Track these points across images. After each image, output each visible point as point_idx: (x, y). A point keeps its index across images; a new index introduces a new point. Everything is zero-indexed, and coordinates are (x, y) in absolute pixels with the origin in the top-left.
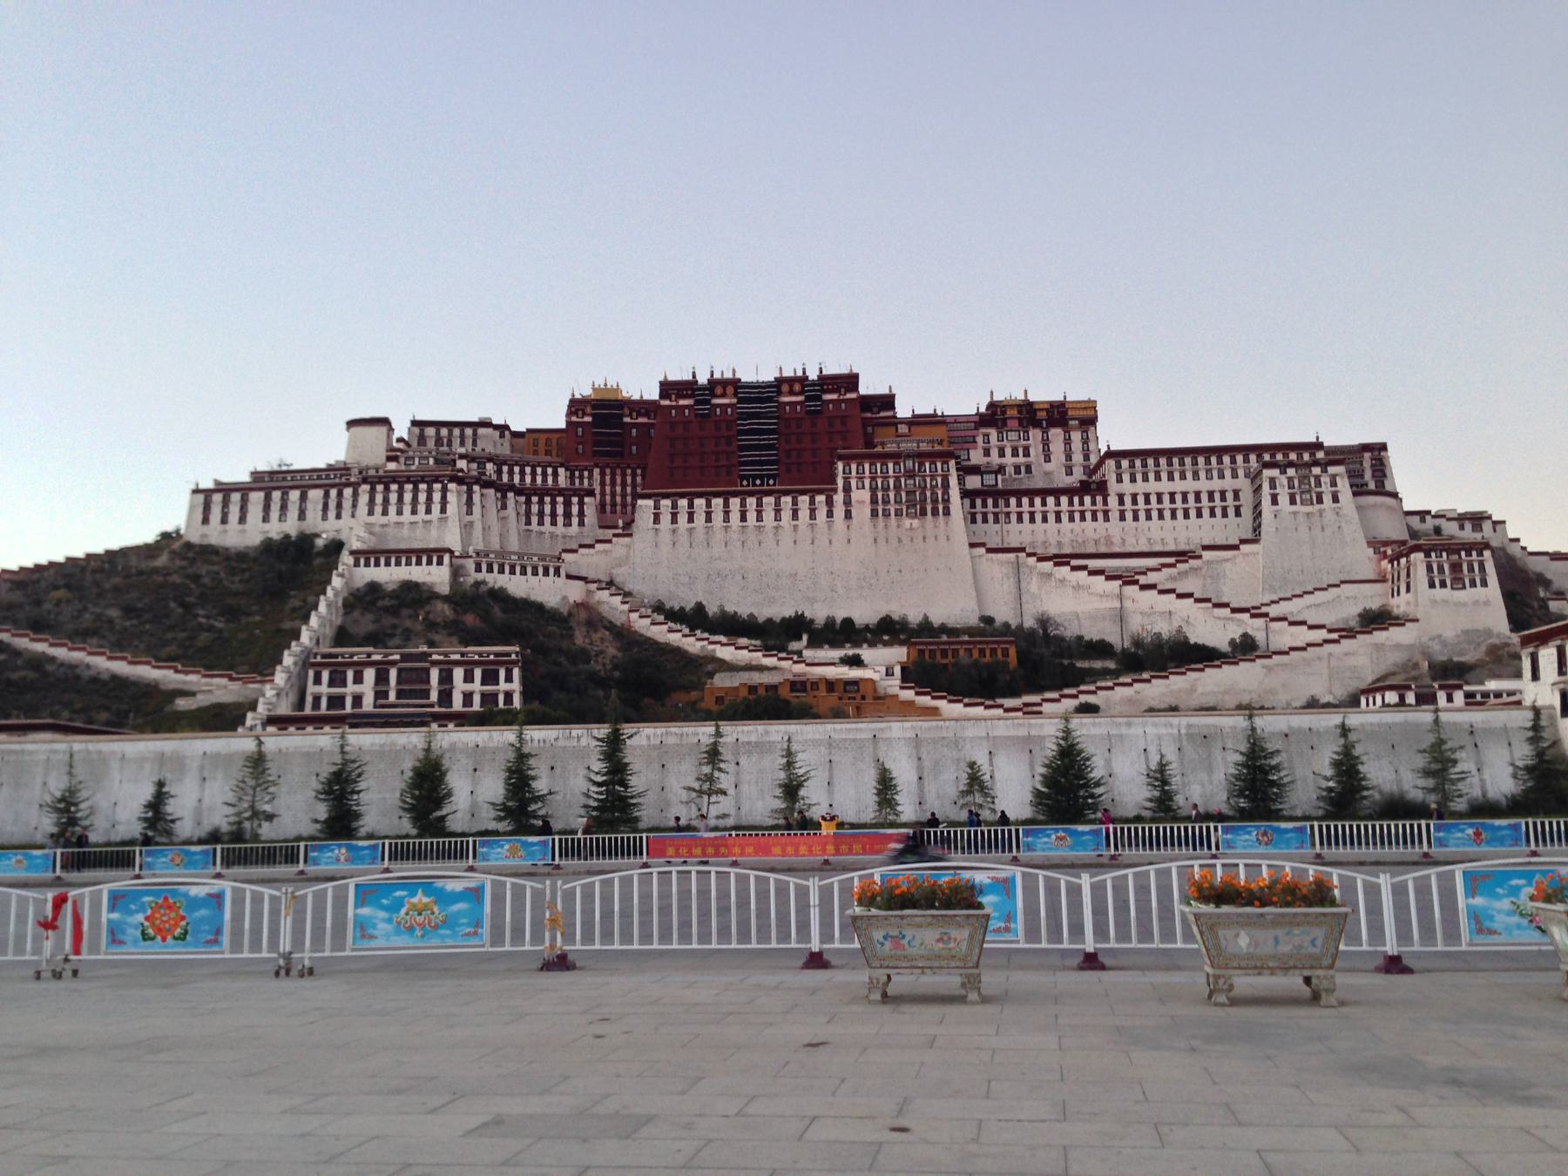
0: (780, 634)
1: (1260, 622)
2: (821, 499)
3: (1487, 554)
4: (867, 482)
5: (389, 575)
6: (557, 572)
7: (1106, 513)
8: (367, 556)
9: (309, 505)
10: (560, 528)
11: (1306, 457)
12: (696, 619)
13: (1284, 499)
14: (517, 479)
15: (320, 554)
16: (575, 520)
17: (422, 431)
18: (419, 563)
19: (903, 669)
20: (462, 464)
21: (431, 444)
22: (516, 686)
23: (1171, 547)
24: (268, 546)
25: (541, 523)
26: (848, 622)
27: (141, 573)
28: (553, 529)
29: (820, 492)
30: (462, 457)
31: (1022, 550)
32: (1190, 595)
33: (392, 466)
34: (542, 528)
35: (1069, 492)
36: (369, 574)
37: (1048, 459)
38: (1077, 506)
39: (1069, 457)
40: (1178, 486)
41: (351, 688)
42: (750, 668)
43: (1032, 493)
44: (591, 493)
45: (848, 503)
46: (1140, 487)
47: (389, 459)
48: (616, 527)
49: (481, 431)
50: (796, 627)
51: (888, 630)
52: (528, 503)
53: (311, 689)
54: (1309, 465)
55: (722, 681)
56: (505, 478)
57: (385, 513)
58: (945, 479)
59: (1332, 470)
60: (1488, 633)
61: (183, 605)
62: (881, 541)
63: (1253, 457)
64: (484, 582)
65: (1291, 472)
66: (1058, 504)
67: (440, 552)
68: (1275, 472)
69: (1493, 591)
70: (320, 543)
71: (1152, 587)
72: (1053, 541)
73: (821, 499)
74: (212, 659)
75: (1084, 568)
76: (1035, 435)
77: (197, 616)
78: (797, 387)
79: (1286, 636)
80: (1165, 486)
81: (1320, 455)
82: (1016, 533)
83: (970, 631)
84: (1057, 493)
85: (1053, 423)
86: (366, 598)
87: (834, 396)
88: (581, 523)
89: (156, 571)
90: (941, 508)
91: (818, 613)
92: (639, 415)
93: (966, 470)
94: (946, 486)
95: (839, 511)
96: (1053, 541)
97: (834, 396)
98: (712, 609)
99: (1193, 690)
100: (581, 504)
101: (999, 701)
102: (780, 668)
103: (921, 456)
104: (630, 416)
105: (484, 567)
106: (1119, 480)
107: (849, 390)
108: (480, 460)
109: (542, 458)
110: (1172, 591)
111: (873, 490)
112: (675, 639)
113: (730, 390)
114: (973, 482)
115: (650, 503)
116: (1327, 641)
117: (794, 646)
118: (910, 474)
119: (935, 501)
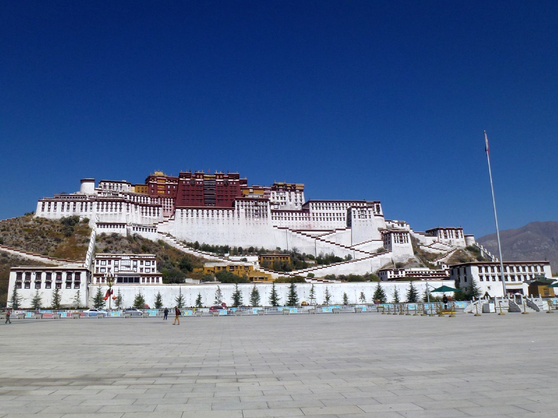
0: (223, 250)
1: (353, 251)
3: (408, 234)
5: (109, 231)
6: (155, 232)
7: (309, 218)
10: (148, 216)
11: (362, 205)
12: (196, 246)
13: (357, 217)
15: (81, 222)
16: (156, 214)
18: (117, 227)
19: (259, 263)
20: (120, 195)
21: (108, 187)
22: (155, 266)
23: (327, 229)
25: (146, 215)
26: (240, 249)
27: (25, 226)
29: (231, 209)
30: (120, 193)
31: (288, 228)
32: (334, 243)
33: (99, 195)
35: (299, 212)
36: (100, 231)
37: (290, 200)
38: (301, 216)
39: (296, 200)
40: (329, 211)
43: (289, 211)
44: (161, 206)
45: (238, 213)
46: (319, 211)
47: (99, 193)
49: (123, 184)
50: (226, 249)
51: (251, 251)
52: (142, 209)
54: (363, 208)
55: (207, 265)
57: (102, 211)
58: (266, 206)
59: (369, 209)
60: (409, 255)
62: (248, 224)
63: (348, 204)
64: (136, 234)
65: (359, 209)
67: (124, 225)
68: (355, 209)
69: (409, 244)
70: (81, 219)
71: (324, 240)
72: (295, 226)
73: (231, 211)
74: (61, 256)
75: (305, 234)
76: (287, 193)
77: (47, 241)
78: (221, 177)
79: (359, 256)
80: (325, 211)
81: (365, 205)
82: (284, 223)
83: (273, 252)
84: (296, 212)
85: (292, 190)
86: (102, 238)
87: (232, 180)
88: (158, 216)
89: (29, 226)
91: (232, 245)
93: (272, 204)
94: (267, 210)
95: (236, 215)
96: (295, 226)
97: (232, 180)
98: (201, 243)
99: (337, 270)
100: (158, 210)
102: (226, 261)
103: (260, 200)
106: (313, 209)
110: (329, 242)
111: (246, 210)
112: (191, 252)
113: (201, 176)
115: (180, 210)
116: (370, 257)
117: (226, 255)
118: (256, 205)
119: (263, 214)
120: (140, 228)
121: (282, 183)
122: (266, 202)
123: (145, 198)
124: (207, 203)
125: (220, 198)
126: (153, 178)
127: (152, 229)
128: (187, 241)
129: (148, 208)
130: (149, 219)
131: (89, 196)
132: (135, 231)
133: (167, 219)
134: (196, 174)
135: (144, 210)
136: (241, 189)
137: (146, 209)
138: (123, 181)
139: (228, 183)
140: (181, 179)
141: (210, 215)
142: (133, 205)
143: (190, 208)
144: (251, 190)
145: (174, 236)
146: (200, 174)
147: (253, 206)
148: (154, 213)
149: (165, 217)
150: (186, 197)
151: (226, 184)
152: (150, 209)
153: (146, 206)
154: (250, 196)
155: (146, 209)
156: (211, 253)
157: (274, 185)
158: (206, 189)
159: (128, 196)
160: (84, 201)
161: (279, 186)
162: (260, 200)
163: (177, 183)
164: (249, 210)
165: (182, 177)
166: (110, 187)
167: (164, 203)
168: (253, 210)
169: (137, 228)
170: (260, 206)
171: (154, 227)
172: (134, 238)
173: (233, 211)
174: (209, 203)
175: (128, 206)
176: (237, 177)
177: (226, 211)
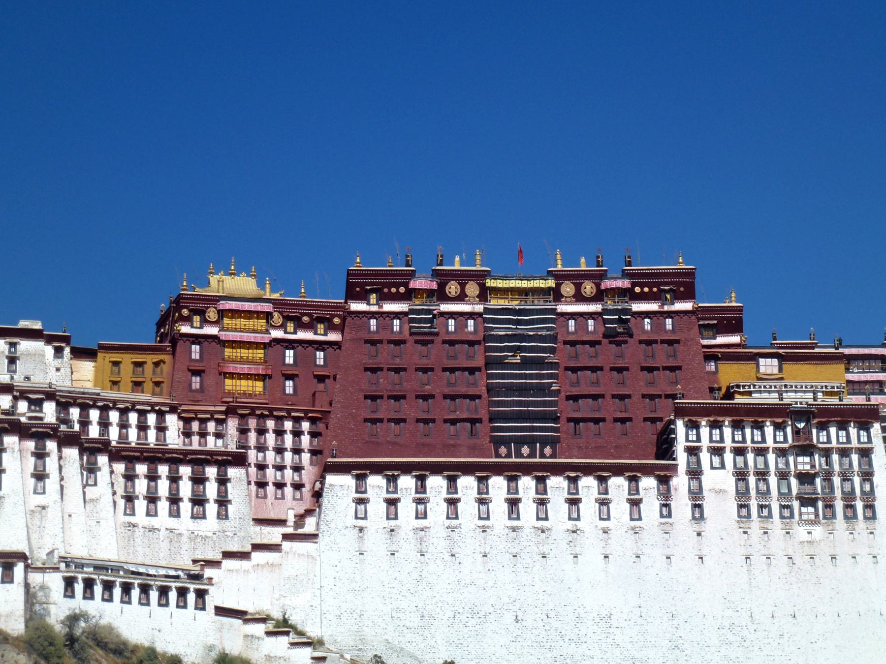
2: (648, 483)
6: (201, 606)
14: (114, 434)
16: (212, 508)
28: (172, 522)
29: (647, 471)
34: (153, 522)
44: (239, 460)
48: (282, 522)
49: (25, 345)
52: (130, 477)
56: (94, 432)
62: (758, 560)
64: (84, 616)
73: (648, 483)
78: (588, 288)
87: (653, 307)
88: (223, 515)
90: (859, 505)
95: (681, 503)
97: (653, 307)
100: (223, 481)
104: (283, 326)
105: (79, 587)
108: (36, 397)
109: (125, 395)
111: (741, 475)
113: (472, 289)
120: (108, 586)
122: (864, 426)
123: (152, 419)
124: (506, 441)
125: (585, 409)
126: (199, 307)
127: (182, 593)
129: (163, 470)
130: (168, 537)
132: (79, 603)
133: (273, 534)
134: (443, 277)
135: (141, 486)
136: (709, 357)
137: (153, 477)
138: (23, 324)
139: (625, 319)
140: (357, 306)
141: (528, 508)
142: (72, 453)
143: (406, 469)
144: (768, 366)
145: (313, 631)
146: (463, 277)
147: (782, 453)
148: (198, 501)
149: (259, 521)
150: (386, 409)
151: (619, 331)
152: (174, 479)
153: (154, 457)
154: (772, 399)
155: (153, 477)
158: (500, 363)
162: (824, 416)
163: (334, 337)
164: (762, 475)
165: (363, 297)
167: (261, 448)
168: (783, 476)
169: (89, 584)
170: (827, 453)
171: (196, 578)
172: (71, 640)
173: (664, 481)
174: (520, 442)
175: (40, 455)
176: (684, 285)
177: (618, 485)
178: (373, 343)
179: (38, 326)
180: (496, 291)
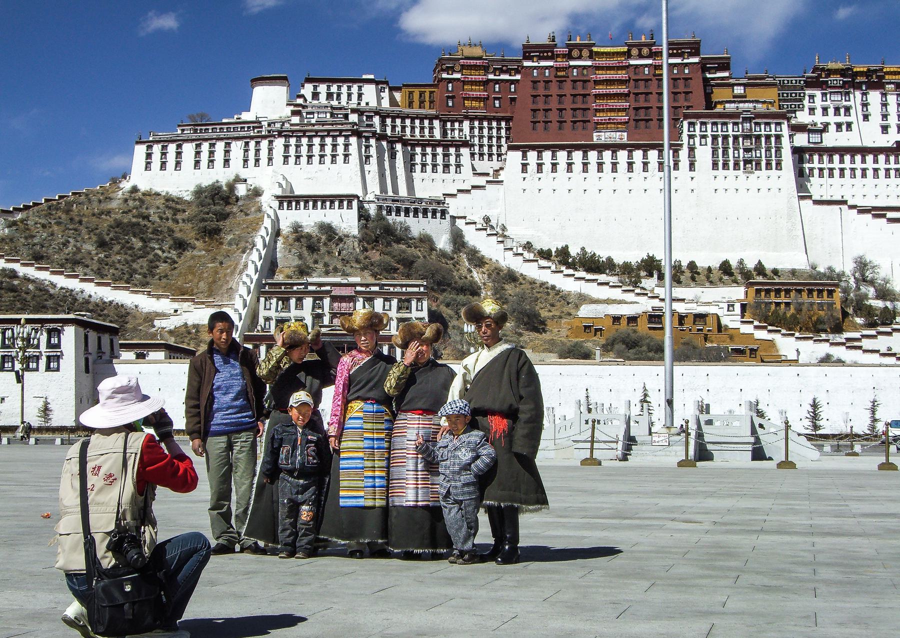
4: (709, 140)
5: (309, 219)
8: (289, 200)
9: (232, 155)
12: (563, 257)
17: (315, 87)
19: (744, 307)
20: (354, 118)
21: (323, 98)
24: (199, 192)
30: (354, 111)
31: (844, 202)
33: (296, 120)
36: (288, 218)
37: (866, 117)
39: (885, 117)
41: (294, 313)
42: (608, 302)
44: (466, 144)
47: (294, 113)
48: (488, 174)
51: (726, 272)
53: (263, 313)
55: (586, 311)
58: (778, 138)
61: (142, 239)
66: (876, 161)
67: (350, 198)
78: (645, 51)
92: (502, 71)
98: (574, 251)
100: (458, 156)
101: (824, 336)
107: (691, 55)
109: (416, 110)
111: (715, 151)
113: (585, 53)
114: (801, 140)
115: (519, 154)
117: (649, 283)
121: (839, 65)
128: (537, 246)
131: (269, 125)
133: (481, 181)
134: (571, 47)
138: (364, 77)
153: (424, 145)
156: (602, 278)
157: (815, 69)
159: (376, 120)
160: (252, 138)
161: (830, 72)
165: (530, 58)
166: (330, 96)
170: (758, 137)
178: (535, 82)
179: (372, 77)
180: (597, 53)
